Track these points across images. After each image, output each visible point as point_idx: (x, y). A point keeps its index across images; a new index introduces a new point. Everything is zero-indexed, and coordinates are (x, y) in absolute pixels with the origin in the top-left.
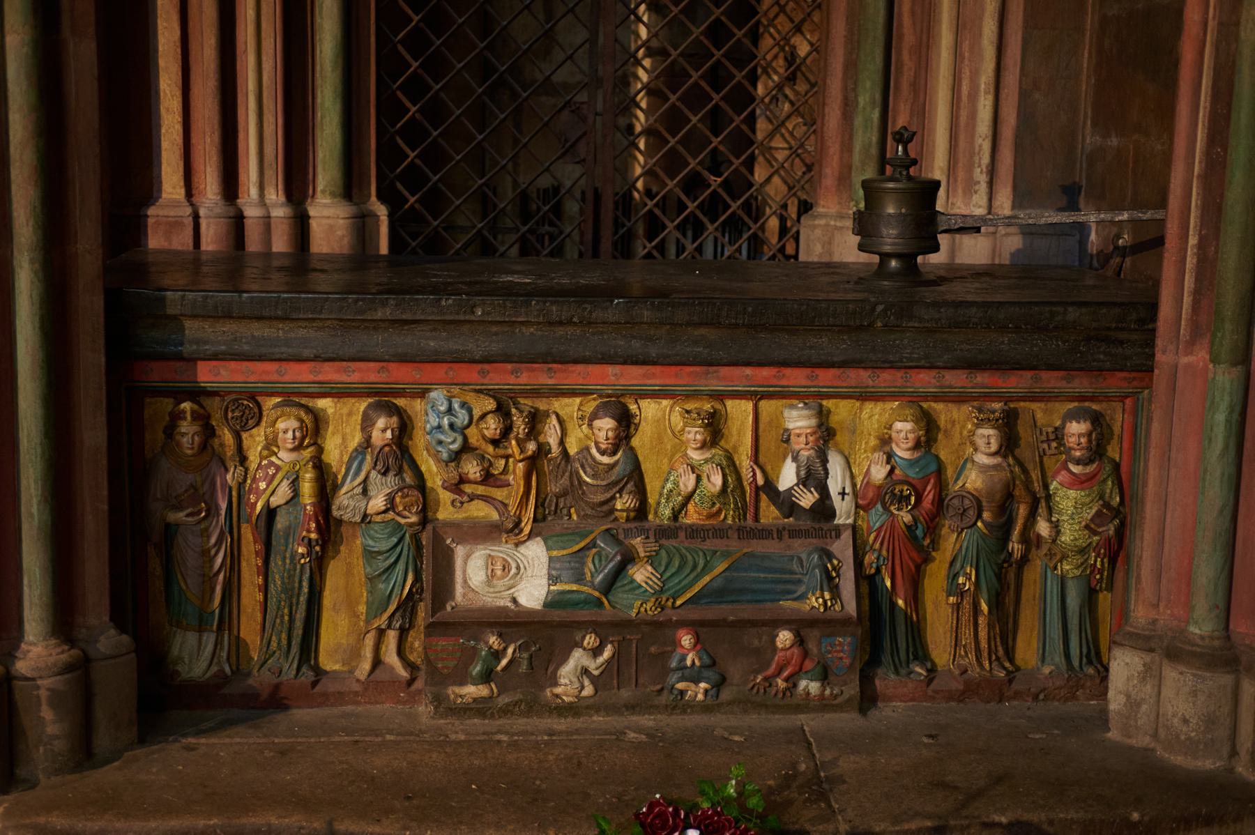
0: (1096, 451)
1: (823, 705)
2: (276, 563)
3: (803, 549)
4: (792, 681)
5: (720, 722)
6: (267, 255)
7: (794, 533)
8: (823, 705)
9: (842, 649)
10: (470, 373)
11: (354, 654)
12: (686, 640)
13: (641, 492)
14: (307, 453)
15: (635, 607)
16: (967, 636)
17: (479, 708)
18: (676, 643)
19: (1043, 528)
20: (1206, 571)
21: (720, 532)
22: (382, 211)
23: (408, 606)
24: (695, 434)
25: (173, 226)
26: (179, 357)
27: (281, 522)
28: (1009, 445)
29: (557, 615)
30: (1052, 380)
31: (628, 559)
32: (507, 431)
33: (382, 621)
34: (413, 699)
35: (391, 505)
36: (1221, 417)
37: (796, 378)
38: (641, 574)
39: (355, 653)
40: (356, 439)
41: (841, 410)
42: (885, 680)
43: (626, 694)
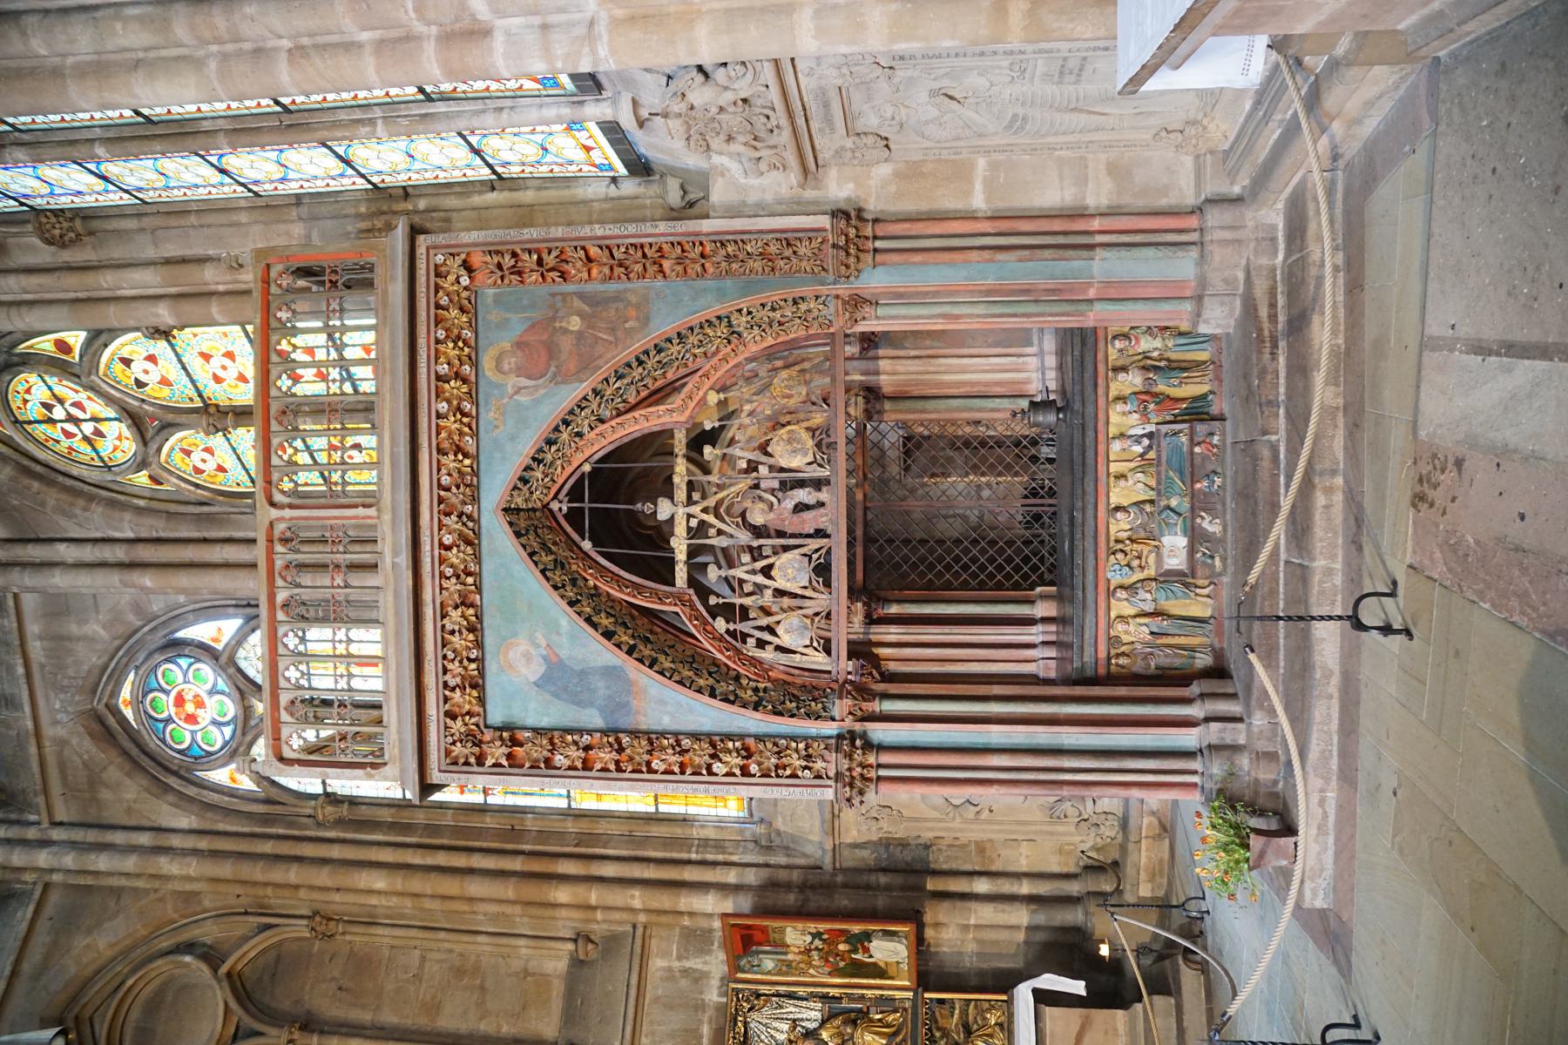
0: (1126, 336)
1: (1223, 434)
2: (1170, 632)
3: (1164, 444)
4: (1214, 446)
5: (1229, 473)
6: (1057, 633)
7: (1159, 446)
8: (1223, 434)
9: (1201, 428)
10: (1101, 563)
11: (1205, 604)
12: (1198, 486)
13: (1143, 502)
14: (1130, 620)
15: (1185, 506)
16: (1198, 380)
17: (1224, 560)
18: (1200, 490)
19: (1155, 354)
20: (1167, 307)
21: (1159, 474)
22: (1039, 589)
23: (1186, 585)
24: (1122, 483)
25: (1047, 668)
26: (1096, 663)
27: (1155, 630)
28: (1124, 369)
29: (1189, 533)
30: (1100, 356)
31: (1168, 508)
32: (1122, 551)
33: (1192, 594)
34: (1222, 584)
35: (1150, 591)
36: (1111, 307)
37: (1102, 448)
38: (1174, 503)
39: (1205, 604)
40: (1125, 603)
41: (1113, 431)
42: (1214, 410)
43: (1219, 507)
